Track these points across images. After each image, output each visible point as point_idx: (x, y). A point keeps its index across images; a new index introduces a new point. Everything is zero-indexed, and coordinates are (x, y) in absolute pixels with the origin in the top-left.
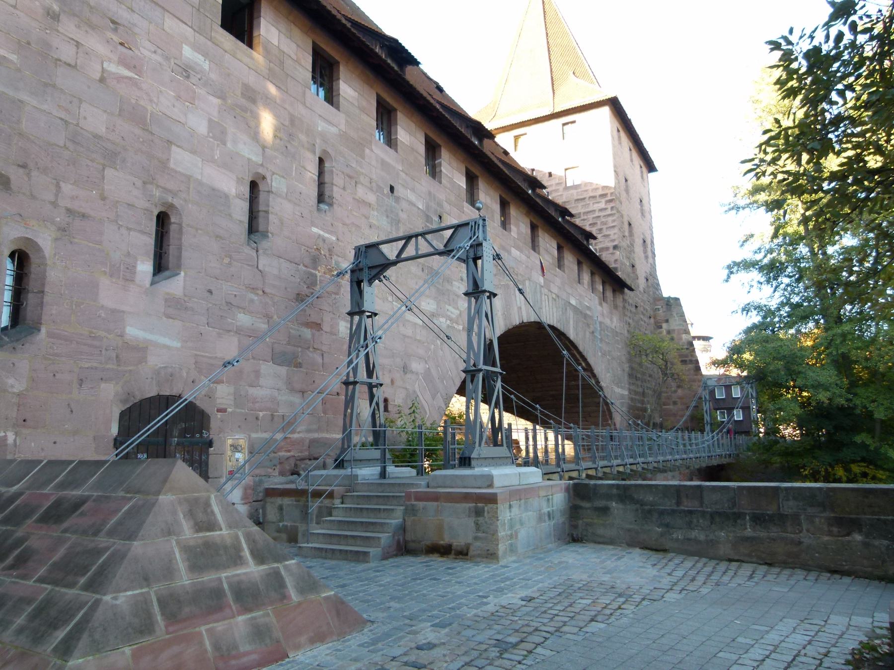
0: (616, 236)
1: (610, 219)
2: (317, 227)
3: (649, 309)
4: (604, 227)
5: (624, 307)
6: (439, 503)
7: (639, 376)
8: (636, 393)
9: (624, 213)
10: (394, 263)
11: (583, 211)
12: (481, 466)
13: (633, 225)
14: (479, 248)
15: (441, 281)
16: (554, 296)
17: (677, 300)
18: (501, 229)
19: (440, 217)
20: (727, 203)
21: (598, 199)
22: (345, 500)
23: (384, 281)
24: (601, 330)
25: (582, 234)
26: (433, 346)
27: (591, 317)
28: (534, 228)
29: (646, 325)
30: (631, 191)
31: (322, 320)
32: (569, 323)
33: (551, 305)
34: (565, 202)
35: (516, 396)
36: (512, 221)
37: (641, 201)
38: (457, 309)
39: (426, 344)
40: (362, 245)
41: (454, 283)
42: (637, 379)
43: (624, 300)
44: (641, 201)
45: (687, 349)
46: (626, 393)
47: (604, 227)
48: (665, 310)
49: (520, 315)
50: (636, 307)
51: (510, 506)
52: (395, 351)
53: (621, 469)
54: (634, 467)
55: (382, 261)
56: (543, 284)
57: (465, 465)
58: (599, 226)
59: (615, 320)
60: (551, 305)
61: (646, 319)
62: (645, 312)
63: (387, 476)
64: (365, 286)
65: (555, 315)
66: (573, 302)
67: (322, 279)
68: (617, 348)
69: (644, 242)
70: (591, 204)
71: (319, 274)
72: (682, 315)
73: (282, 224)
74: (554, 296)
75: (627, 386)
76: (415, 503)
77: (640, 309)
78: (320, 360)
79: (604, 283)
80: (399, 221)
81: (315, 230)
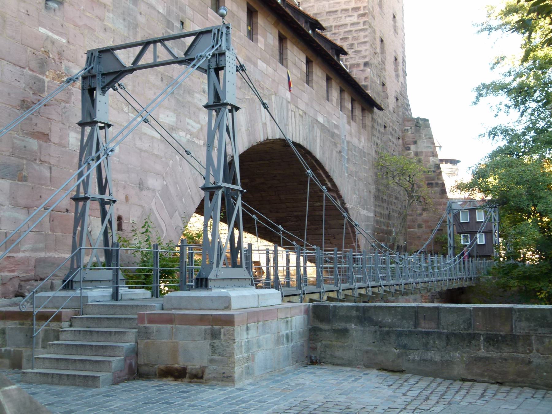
0: (368, 52)
1: (362, 34)
2: (45, 28)
3: (398, 130)
4: (356, 42)
5: (373, 127)
6: (174, 326)
7: (385, 197)
8: (381, 215)
9: (376, 28)
10: (130, 71)
11: (334, 24)
12: (219, 287)
13: (385, 42)
14: (222, 58)
15: (181, 92)
16: (301, 113)
17: (426, 121)
18: (247, 39)
19: (182, 23)
20: (480, 23)
21: (351, 13)
22: (73, 324)
23: (119, 90)
24: (348, 150)
25: (332, 49)
26: (171, 162)
27: (339, 136)
28: (282, 39)
29: (394, 146)
30: (385, 6)
31: (50, 129)
32: (316, 141)
33: (297, 121)
34: (316, 14)
35: (258, 216)
36: (260, 31)
37: (394, 17)
38: (198, 122)
39: (164, 159)
40: (95, 50)
41: (196, 95)
42: (383, 201)
43: (373, 120)
44: (394, 17)
45: (434, 172)
46: (371, 215)
47: (356, 42)
48: (413, 131)
49: (265, 132)
50: (385, 127)
51: (248, 329)
52: (130, 166)
53: (363, 291)
54: (376, 290)
55: (118, 68)
56: (289, 100)
57: (201, 286)
58: (350, 42)
59: (363, 140)
60: (297, 121)
61: (394, 140)
62: (393, 132)
63: (120, 298)
64: (97, 94)
65: (301, 132)
66: (321, 119)
67: (51, 85)
68: (364, 168)
69: (396, 59)
70: (343, 18)
71: (47, 80)
72: (431, 137)
73: (4, 21)
74: (301, 113)
75: (373, 208)
76: (148, 325)
77: (389, 129)
78: (48, 174)
79: (353, 101)
80: (137, 25)
81: (42, 30)
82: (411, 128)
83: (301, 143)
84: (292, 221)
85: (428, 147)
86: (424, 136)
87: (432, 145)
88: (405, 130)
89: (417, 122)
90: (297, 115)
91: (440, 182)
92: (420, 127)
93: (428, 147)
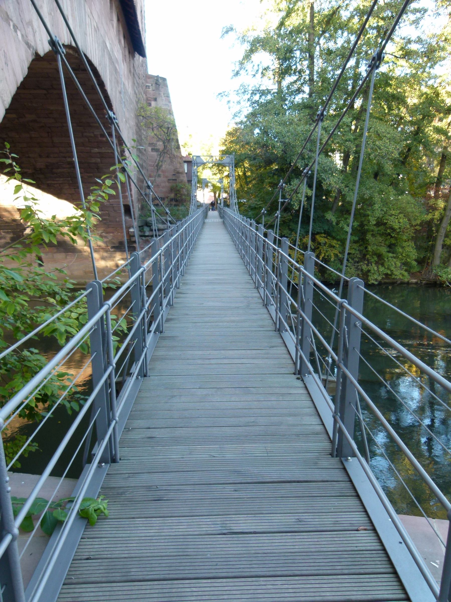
5: (134, 75)
17: (164, 80)
48: (154, 88)
59: (130, 85)
72: (168, 96)
82: (152, 85)
83: (98, 68)
84: (64, 168)
85: (166, 105)
86: (162, 94)
87: (169, 104)
88: (147, 86)
89: (157, 80)
90: (93, 27)
91: (174, 137)
92: (159, 85)
93: (166, 105)
